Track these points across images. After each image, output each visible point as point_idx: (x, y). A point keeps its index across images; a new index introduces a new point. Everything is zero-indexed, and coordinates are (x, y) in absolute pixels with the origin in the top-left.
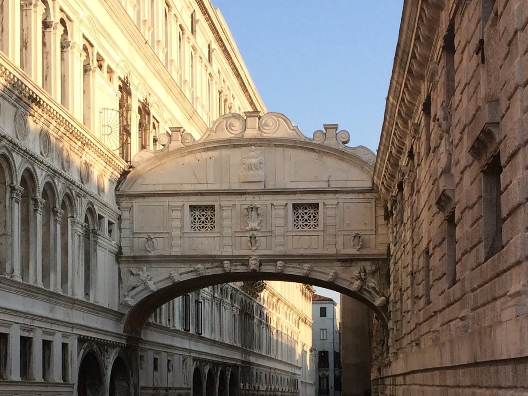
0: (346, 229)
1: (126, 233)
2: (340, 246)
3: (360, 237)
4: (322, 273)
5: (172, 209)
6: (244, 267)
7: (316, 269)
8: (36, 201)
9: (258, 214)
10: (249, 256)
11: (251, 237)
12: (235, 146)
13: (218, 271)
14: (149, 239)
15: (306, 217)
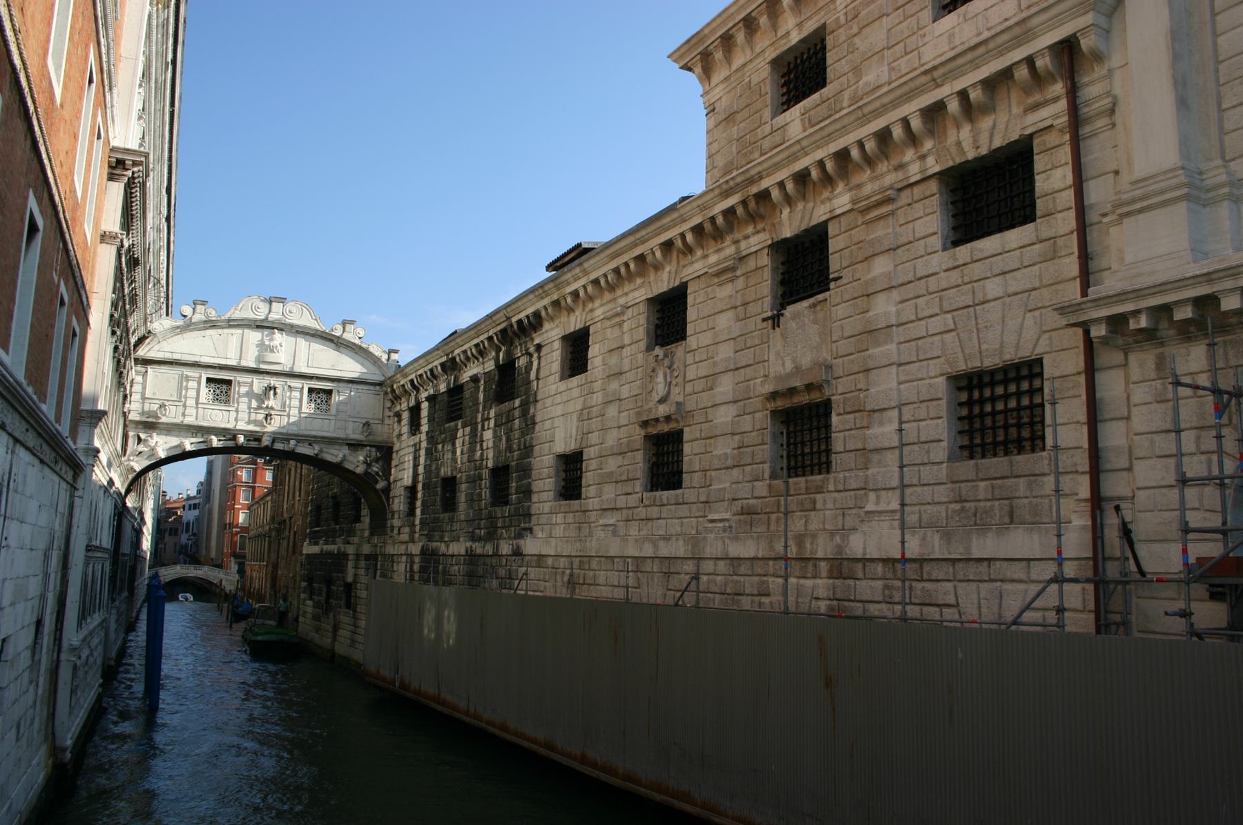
0: (357, 416)
1: (136, 397)
2: (350, 431)
3: (369, 425)
4: (332, 454)
5: (188, 379)
6: (257, 443)
7: (325, 450)
8: (119, 361)
9: (275, 394)
10: (264, 433)
11: (267, 415)
12: (258, 327)
13: (231, 444)
14: (162, 406)
15: (319, 401)
